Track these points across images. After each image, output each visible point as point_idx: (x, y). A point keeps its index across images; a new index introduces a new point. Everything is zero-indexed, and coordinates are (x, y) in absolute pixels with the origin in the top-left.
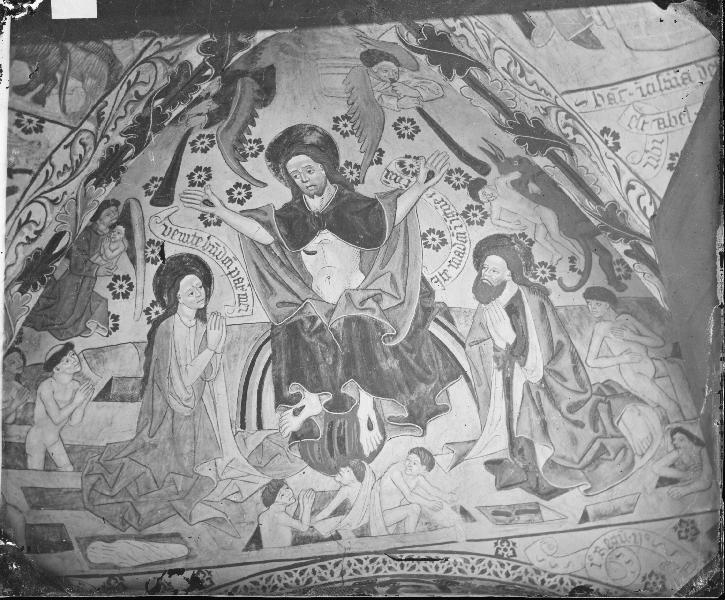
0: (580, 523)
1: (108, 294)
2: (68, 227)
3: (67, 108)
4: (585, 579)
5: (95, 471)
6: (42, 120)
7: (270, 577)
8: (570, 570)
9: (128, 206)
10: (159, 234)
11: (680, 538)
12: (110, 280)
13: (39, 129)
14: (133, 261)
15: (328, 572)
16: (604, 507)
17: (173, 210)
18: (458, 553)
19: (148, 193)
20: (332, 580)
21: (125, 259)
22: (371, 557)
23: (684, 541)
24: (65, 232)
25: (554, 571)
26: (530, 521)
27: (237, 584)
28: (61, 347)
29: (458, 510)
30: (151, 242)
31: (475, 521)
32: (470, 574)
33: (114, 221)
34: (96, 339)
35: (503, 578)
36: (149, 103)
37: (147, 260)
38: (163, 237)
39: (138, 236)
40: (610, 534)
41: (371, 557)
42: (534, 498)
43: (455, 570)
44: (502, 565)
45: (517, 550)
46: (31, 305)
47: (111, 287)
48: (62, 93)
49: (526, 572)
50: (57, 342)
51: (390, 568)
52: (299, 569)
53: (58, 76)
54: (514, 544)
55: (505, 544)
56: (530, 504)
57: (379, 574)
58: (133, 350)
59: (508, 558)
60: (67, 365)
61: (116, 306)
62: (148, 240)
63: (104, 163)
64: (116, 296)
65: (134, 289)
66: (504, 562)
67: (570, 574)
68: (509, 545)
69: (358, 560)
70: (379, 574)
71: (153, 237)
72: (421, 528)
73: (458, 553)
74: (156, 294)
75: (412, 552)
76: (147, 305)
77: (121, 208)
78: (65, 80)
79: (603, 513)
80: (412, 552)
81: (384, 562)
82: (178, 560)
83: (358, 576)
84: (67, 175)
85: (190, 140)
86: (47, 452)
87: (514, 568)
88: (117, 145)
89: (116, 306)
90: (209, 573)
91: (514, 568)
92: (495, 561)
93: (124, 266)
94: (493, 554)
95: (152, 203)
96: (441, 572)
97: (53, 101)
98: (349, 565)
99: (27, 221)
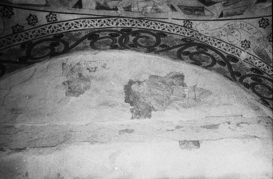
0: (219, 17)
4: (219, 40)
7: (85, 21)
8: (213, 35)
11: (260, 26)
15: (111, 22)
16: (230, 11)
18: (168, 23)
20: (112, 26)
22: (131, 19)
23: (261, 28)
25: (207, 35)
26: (199, 15)
27: (68, 22)
29: (170, 6)
31: (176, 11)
32: (172, 32)
35: (186, 35)
40: (231, 23)
41: (131, 19)
42: (201, 5)
43: (166, 29)
44: (186, 30)
45: (192, 25)
49: (196, 34)
51: (139, 25)
52: (98, 20)
54: (192, 23)
55: (188, 22)
56: (200, 7)
57: (134, 27)
59: (189, 28)
66: (187, 29)
67: (213, 37)
68: (189, 23)
69: (125, 20)
70: (134, 27)
72: (153, 11)
73: (168, 23)
75: (148, 20)
79: (230, 14)
80: (148, 20)
81: (136, 22)
82: (42, 6)
83: (123, 26)
87: (191, 32)
90: (55, 15)
91: (191, 32)
92: (183, 28)
94: (183, 25)
96: (160, 29)
98: (121, 21)
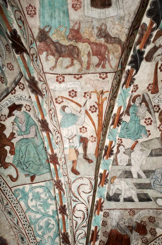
1: (145, 125)
2: (122, 104)
3: (112, 66)
5: (154, 178)
6: (106, 73)
9: (143, 96)
10: (157, 103)
12: (144, 120)
13: (107, 77)
14: (150, 113)
17: (159, 94)
19: (149, 90)
21: (147, 113)
24: (121, 106)
28: (135, 142)
30: (155, 106)
33: (141, 102)
34: (144, 139)
36: (135, 49)
37: (155, 112)
38: (158, 104)
39: (150, 106)
46: (119, 131)
47: (145, 122)
48: (109, 62)
50: (133, 141)
53: (106, 56)
58: (157, 140)
60: (137, 148)
61: (148, 128)
62: (153, 105)
63: (126, 79)
64: (148, 125)
65: (153, 121)
71: (155, 104)
74: (160, 122)
76: (158, 126)
77: (141, 97)
78: (108, 57)
84: (117, 86)
85: (158, 67)
86: (138, 173)
88: (128, 70)
89: (148, 128)
93: (148, 115)
95: (152, 93)
97: (107, 65)
99: (111, 106)
